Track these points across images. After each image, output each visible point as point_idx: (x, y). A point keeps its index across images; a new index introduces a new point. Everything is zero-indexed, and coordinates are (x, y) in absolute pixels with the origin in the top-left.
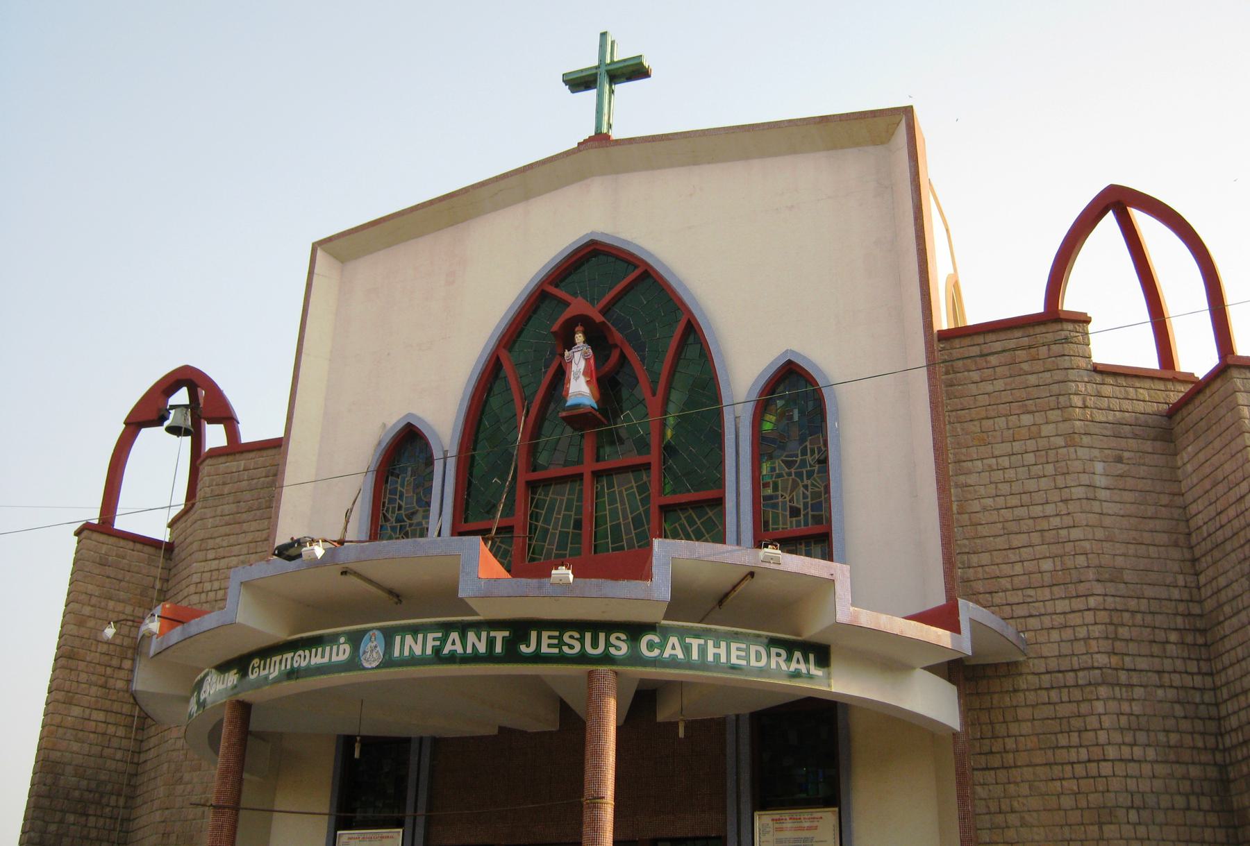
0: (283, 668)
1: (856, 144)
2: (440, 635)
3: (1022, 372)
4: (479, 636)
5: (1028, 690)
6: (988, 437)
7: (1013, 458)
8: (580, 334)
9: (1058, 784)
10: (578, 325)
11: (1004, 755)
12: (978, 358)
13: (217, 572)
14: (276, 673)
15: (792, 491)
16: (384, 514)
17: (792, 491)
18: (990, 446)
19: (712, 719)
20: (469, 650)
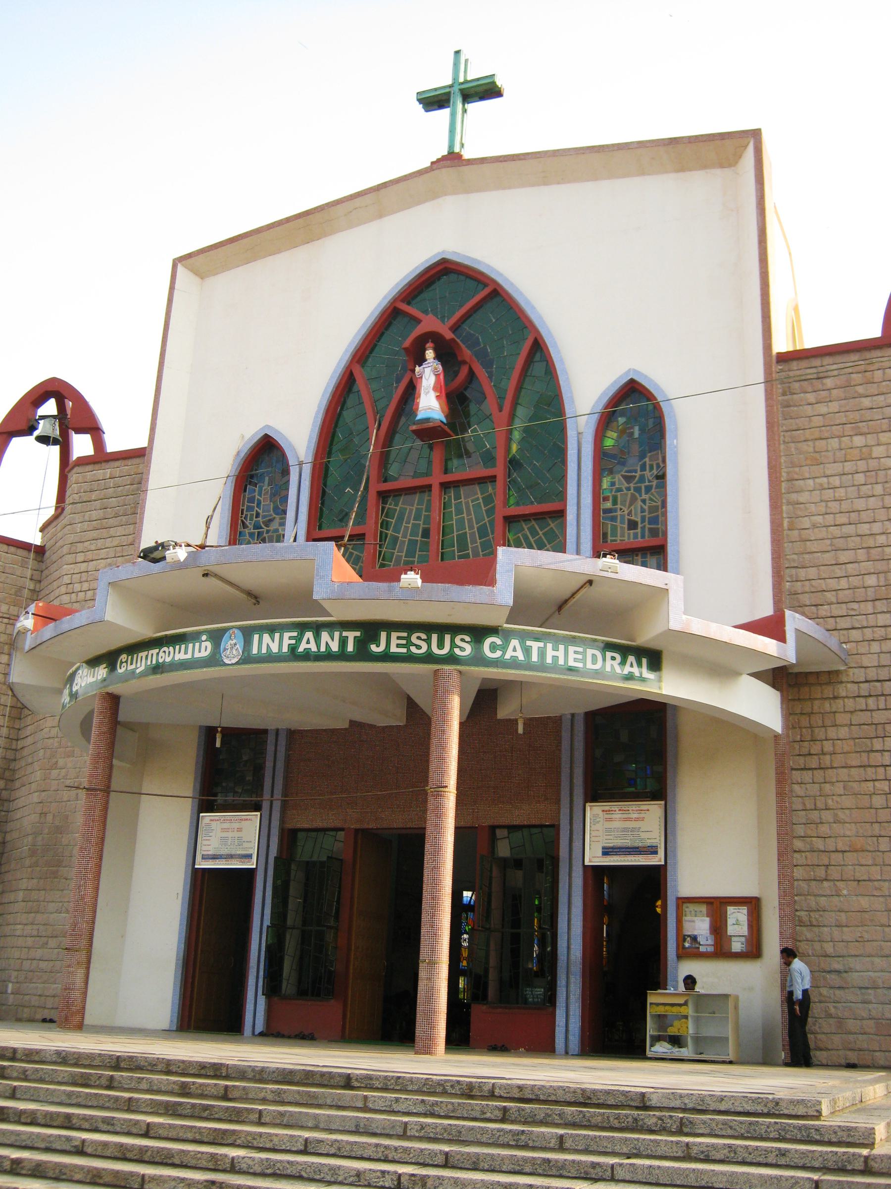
0: (149, 663)
1: (704, 166)
2: (295, 634)
3: (856, 395)
4: (332, 635)
5: (847, 697)
6: (821, 457)
7: (844, 477)
8: (431, 351)
9: (870, 784)
10: (428, 342)
11: (821, 757)
12: (814, 381)
13: (86, 574)
14: (143, 668)
15: (630, 505)
16: (242, 521)
17: (630, 505)
18: (822, 466)
19: (549, 718)
20: (323, 649)
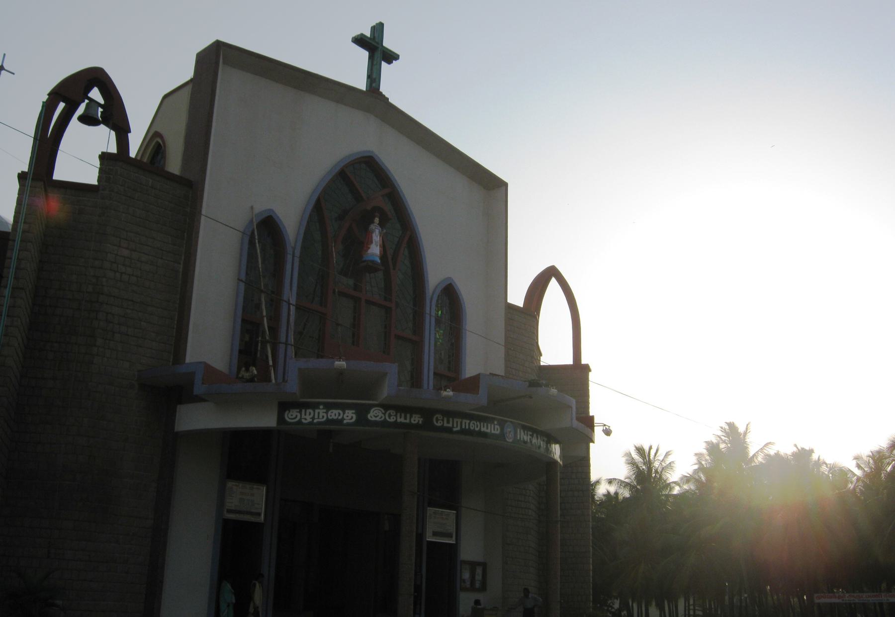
14: (459, 428)
